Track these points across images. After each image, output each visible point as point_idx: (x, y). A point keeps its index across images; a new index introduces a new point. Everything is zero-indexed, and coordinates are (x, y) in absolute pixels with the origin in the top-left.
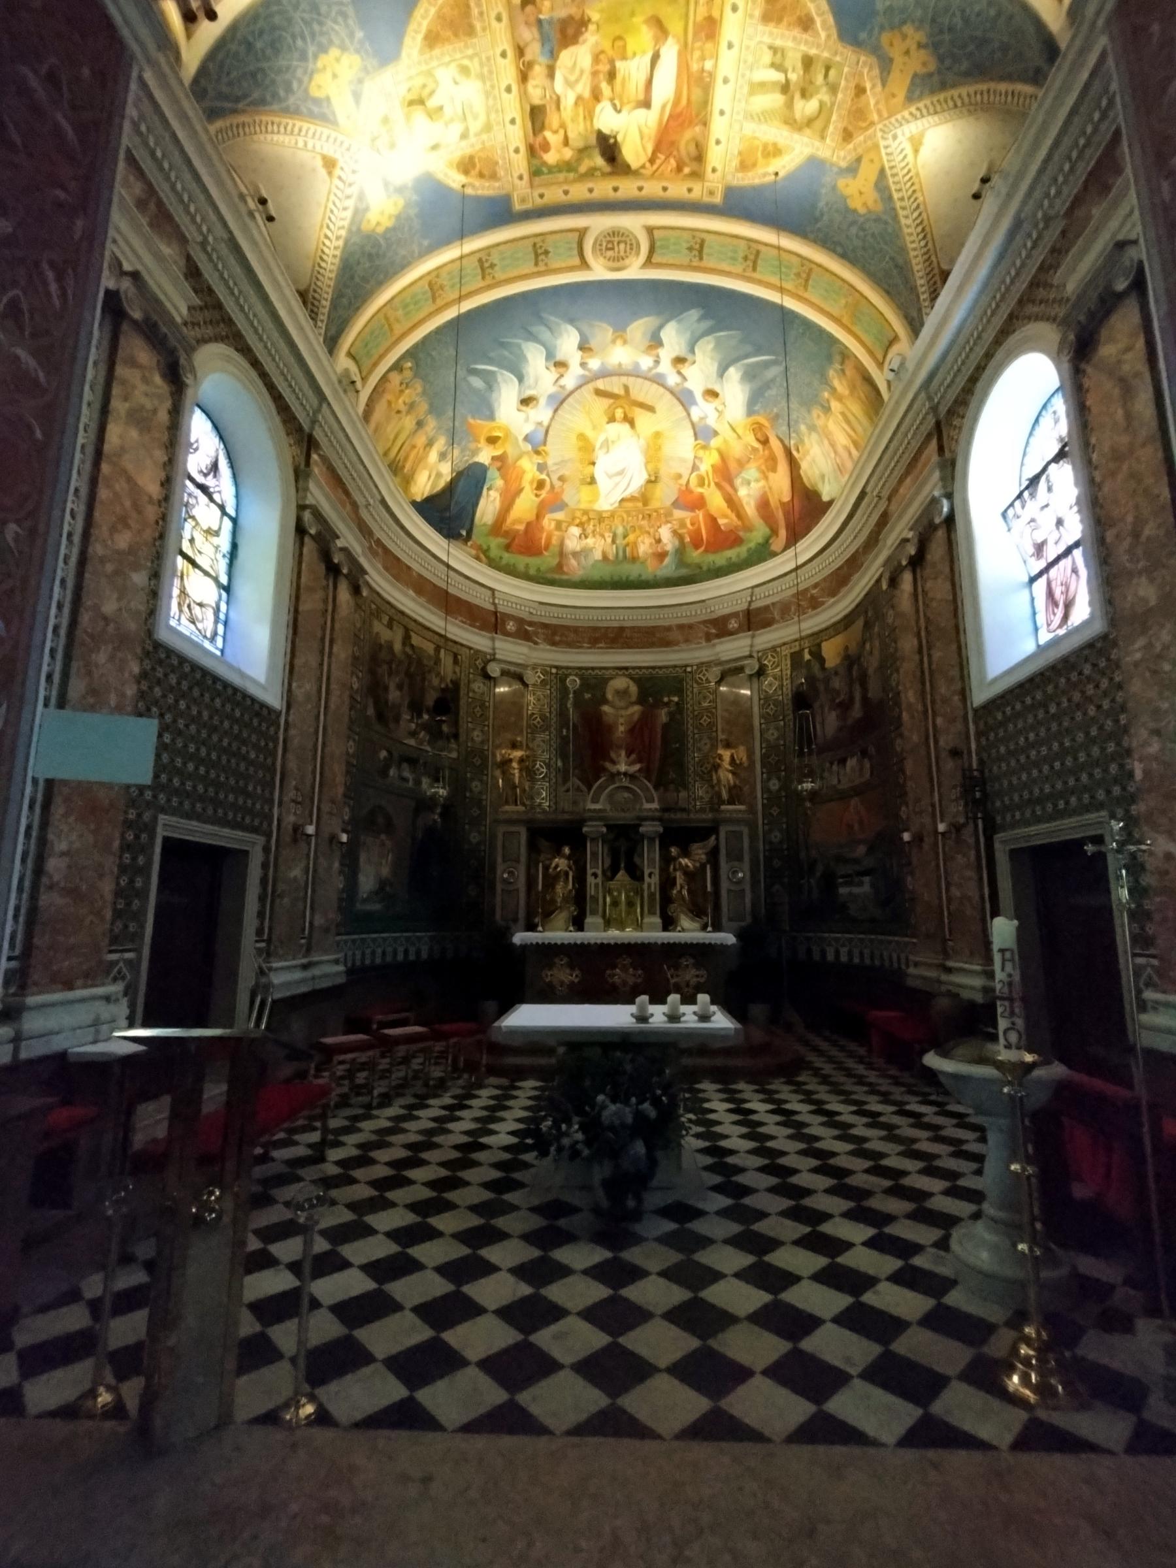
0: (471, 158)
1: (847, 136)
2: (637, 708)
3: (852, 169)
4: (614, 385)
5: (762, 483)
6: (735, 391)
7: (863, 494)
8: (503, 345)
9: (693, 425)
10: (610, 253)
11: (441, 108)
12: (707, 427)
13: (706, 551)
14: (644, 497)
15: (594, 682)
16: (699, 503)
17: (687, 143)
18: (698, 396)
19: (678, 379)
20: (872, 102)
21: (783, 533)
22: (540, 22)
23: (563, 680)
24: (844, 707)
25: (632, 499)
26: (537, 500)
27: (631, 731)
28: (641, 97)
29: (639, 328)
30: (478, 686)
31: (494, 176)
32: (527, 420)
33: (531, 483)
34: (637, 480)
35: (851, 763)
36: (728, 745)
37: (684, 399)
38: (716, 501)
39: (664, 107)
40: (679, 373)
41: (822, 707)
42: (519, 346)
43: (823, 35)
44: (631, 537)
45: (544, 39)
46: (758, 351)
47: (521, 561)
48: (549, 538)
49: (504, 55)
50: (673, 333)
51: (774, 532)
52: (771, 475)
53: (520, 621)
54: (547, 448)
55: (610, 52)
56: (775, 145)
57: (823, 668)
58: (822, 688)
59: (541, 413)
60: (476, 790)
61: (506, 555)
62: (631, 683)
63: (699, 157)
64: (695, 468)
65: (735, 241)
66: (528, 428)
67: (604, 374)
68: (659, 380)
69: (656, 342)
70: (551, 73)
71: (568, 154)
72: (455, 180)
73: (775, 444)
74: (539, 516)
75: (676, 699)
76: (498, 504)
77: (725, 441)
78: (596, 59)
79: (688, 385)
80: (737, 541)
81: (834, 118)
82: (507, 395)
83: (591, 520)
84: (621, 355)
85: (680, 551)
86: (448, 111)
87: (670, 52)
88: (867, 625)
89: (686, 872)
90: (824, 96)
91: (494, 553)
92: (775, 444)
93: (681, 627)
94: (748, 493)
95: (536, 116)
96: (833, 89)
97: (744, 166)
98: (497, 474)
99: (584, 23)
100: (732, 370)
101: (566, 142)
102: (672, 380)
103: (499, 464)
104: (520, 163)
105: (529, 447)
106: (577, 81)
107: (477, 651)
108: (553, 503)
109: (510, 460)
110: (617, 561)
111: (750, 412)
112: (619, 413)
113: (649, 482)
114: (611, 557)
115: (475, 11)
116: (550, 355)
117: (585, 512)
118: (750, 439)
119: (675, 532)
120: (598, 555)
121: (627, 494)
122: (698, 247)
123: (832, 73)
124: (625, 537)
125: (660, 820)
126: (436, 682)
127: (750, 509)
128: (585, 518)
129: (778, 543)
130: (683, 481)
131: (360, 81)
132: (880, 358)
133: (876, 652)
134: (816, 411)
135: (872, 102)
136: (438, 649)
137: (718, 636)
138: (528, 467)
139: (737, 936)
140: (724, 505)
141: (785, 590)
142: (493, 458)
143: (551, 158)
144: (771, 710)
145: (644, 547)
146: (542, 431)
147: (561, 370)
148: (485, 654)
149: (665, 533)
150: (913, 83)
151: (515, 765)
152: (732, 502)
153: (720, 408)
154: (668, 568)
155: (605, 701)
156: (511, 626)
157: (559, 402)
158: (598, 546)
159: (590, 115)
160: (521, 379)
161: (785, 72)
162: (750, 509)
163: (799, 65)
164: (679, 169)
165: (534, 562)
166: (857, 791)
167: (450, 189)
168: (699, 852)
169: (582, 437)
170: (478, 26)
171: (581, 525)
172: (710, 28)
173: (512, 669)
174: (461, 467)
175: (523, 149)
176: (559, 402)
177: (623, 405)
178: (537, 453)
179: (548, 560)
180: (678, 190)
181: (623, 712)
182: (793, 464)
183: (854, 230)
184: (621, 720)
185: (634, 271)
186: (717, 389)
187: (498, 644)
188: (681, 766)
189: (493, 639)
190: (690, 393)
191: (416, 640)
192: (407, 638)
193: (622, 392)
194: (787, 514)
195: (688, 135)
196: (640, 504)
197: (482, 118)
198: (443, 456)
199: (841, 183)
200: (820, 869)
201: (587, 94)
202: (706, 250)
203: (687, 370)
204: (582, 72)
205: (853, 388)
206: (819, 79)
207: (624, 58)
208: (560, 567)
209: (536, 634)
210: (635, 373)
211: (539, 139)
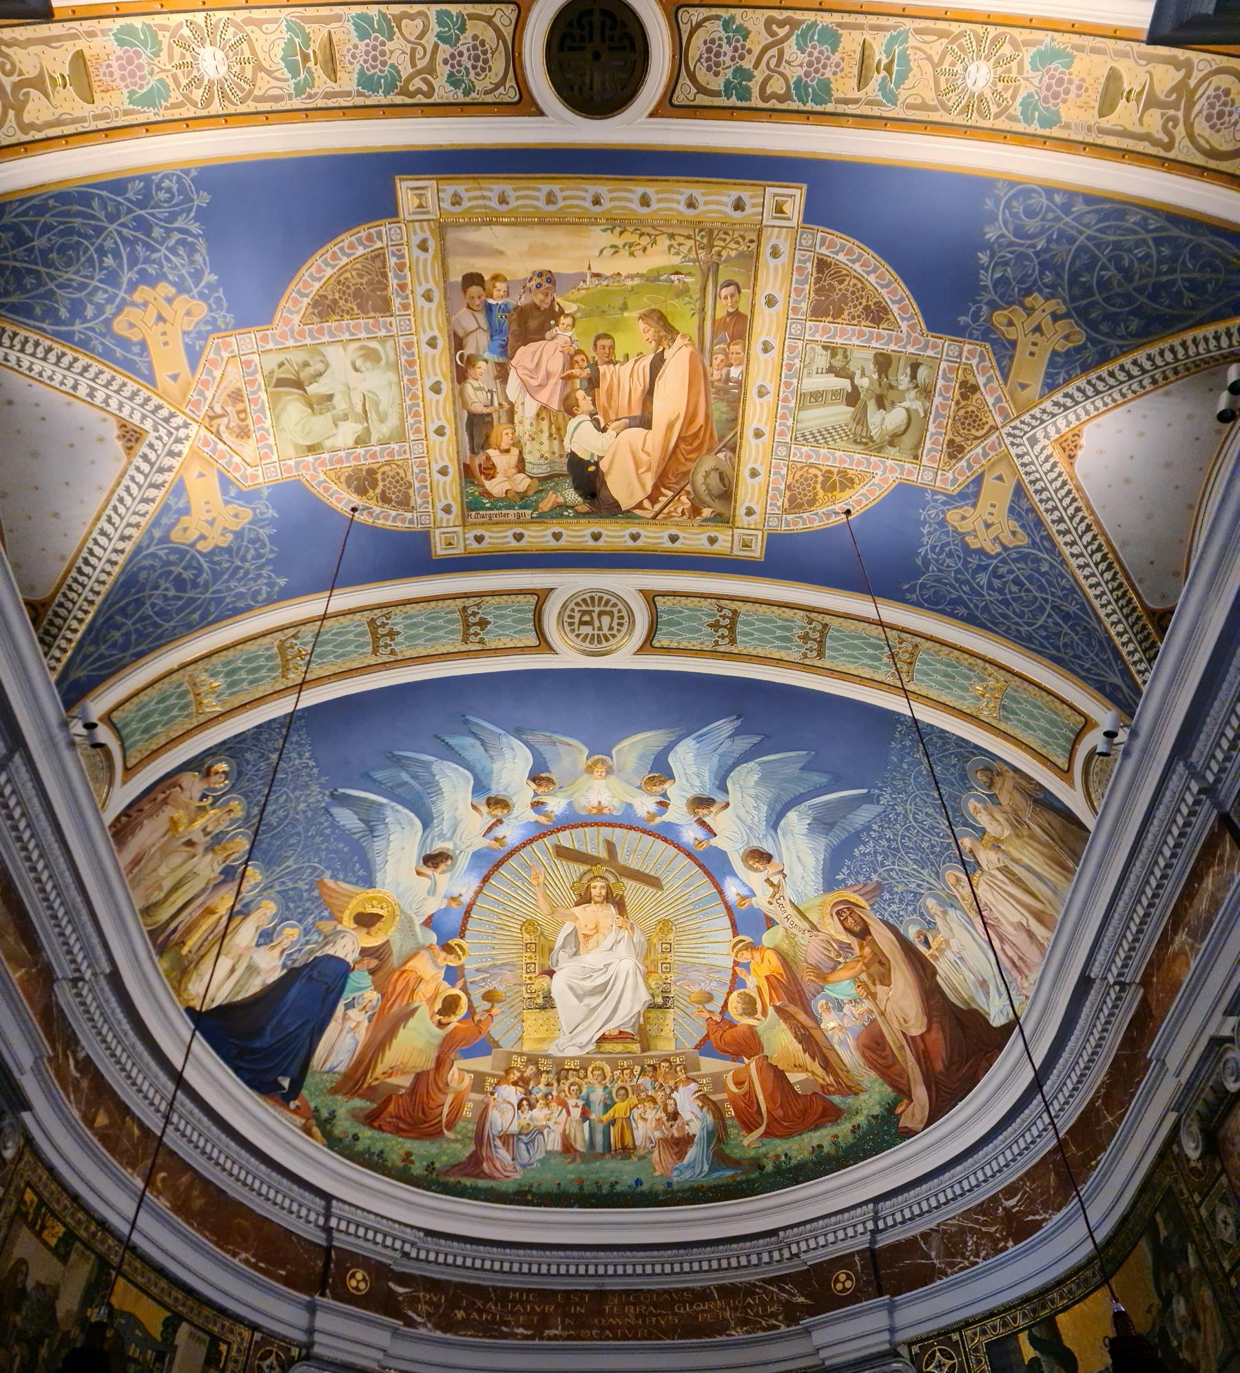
0: (371, 472)
1: (955, 450)
3: (971, 494)
4: (590, 841)
5: (867, 1004)
6: (800, 851)
7: (1085, 982)
8: (399, 762)
9: (729, 909)
10: (585, 630)
11: (330, 397)
12: (754, 912)
13: (766, 1134)
14: (642, 1035)
16: (746, 1046)
17: (707, 475)
19: (700, 833)
20: (990, 400)
21: (920, 1093)
22: (489, 309)
25: (622, 1036)
26: (442, 1033)
28: (637, 412)
29: (634, 748)
31: (405, 503)
32: (432, 891)
34: (630, 1003)
37: (712, 866)
38: (780, 1041)
39: (670, 426)
40: (702, 823)
42: (426, 765)
43: (904, 326)
44: (620, 1109)
45: (494, 331)
46: (838, 782)
47: (396, 1146)
49: (432, 343)
50: (690, 757)
51: (903, 1092)
52: (880, 990)
53: (379, 1271)
55: (591, 353)
56: (843, 473)
59: (458, 882)
61: (366, 1133)
63: (727, 495)
64: (736, 982)
65: (789, 613)
66: (433, 906)
67: (571, 822)
68: (666, 834)
69: (660, 771)
70: (502, 374)
71: (522, 483)
72: (342, 499)
73: (882, 936)
74: (441, 1063)
76: (362, 1035)
77: (788, 936)
78: (571, 361)
80: (832, 1114)
81: (932, 428)
82: (400, 845)
83: (541, 1075)
84: (601, 793)
85: (717, 1135)
86: (340, 403)
87: (678, 359)
88: (1166, 1260)
90: (913, 402)
92: (882, 936)
93: (727, 1291)
94: (840, 1027)
95: (478, 428)
96: (926, 392)
97: (795, 505)
98: (367, 980)
99: (554, 314)
100: (792, 816)
101: (521, 466)
102: (691, 835)
103: (374, 963)
104: (449, 489)
105: (433, 938)
106: (541, 386)
107: (270, 1336)
108: (473, 1041)
109: (395, 961)
110: (592, 1153)
111: (830, 883)
112: (598, 889)
113: (652, 1006)
114: (580, 1146)
115: (393, 282)
116: (479, 787)
117: (533, 1060)
118: (834, 929)
119: (704, 1099)
120: (553, 1142)
122: (727, 622)
123: (922, 373)
124: (607, 1107)
127: (849, 1055)
128: (530, 1071)
130: (716, 1006)
131: (203, 336)
132: (1062, 762)
133: (1211, 1322)
135: (990, 400)
136: (171, 1325)
137: (813, 1311)
138: (428, 971)
142: (364, 952)
143: (496, 487)
145: (646, 1128)
146: (458, 912)
147: (498, 812)
148: (287, 1342)
149: (686, 1100)
150: (1051, 363)
152: (810, 1041)
153: (775, 880)
156: (358, 1281)
157: (492, 864)
158: (555, 1123)
159: (558, 433)
160: (427, 822)
161: (852, 378)
162: (849, 1055)
163: (871, 367)
164: (695, 511)
167: (332, 511)
169: (530, 925)
170: (396, 303)
171: (522, 1082)
172: (738, 326)
174: (301, 960)
175: (453, 470)
176: (492, 864)
177: (606, 880)
178: (448, 949)
179: (453, 1148)
180: (694, 540)
182: (923, 970)
183: (983, 578)
185: (624, 656)
187: (323, 1321)
189: (312, 1309)
190: (722, 855)
192: (98, 1288)
193: (603, 853)
194: (924, 1058)
195: (708, 463)
196: (636, 1048)
197: (393, 421)
198: (266, 937)
199: (953, 517)
201: (555, 405)
202: (740, 628)
204: (548, 375)
205: (1017, 823)
206: (904, 382)
207: (611, 362)
208: (474, 1164)
209: (413, 1301)
210: (627, 823)
211: (480, 459)
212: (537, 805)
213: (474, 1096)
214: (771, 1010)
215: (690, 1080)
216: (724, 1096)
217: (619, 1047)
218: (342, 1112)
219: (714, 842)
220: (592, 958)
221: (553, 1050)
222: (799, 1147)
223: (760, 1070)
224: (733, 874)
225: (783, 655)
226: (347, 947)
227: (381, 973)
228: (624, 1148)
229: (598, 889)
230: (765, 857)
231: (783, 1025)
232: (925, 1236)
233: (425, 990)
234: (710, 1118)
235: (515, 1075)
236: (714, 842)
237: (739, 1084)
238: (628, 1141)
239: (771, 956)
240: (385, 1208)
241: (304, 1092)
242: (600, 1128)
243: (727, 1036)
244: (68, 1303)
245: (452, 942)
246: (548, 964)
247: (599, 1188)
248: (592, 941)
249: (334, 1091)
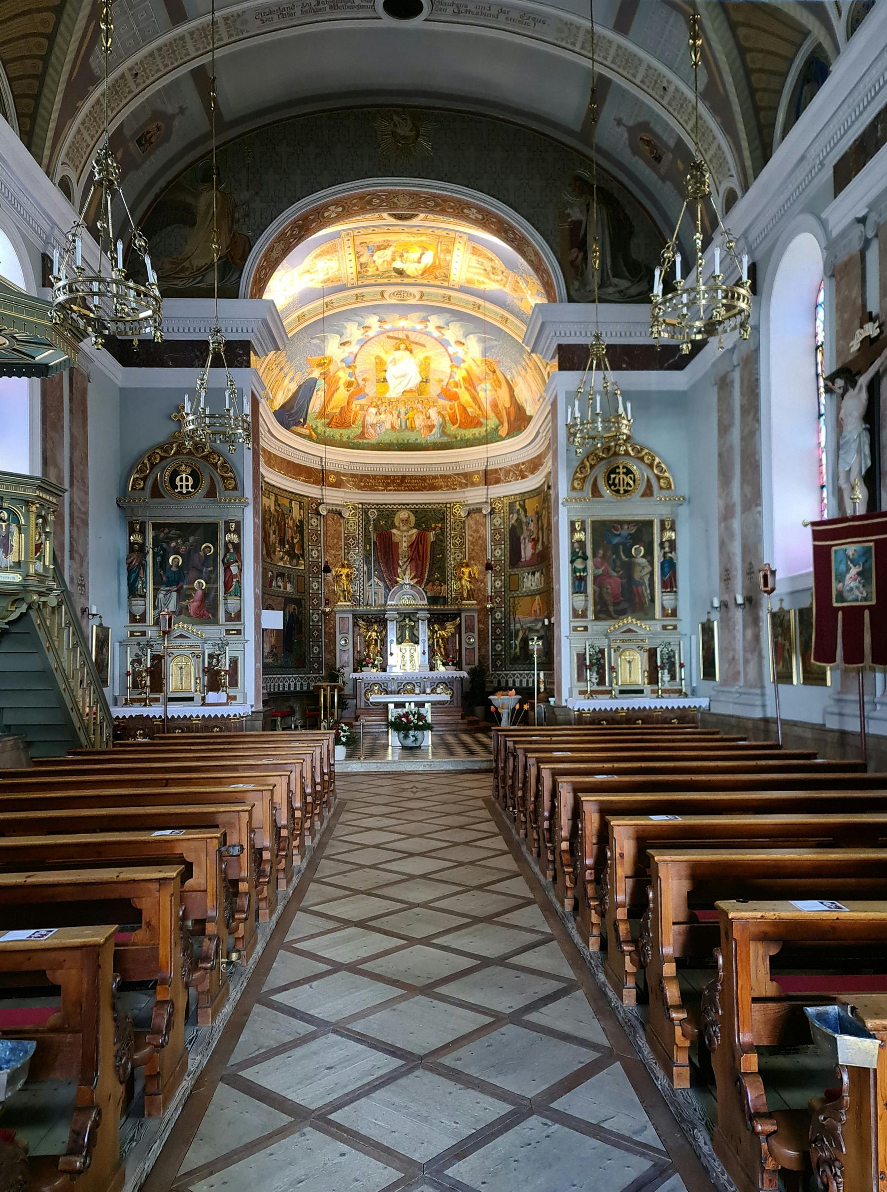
2: (415, 531)
4: (401, 335)
5: (494, 392)
9: (450, 355)
12: (457, 358)
13: (459, 427)
15: (387, 514)
16: (455, 397)
18: (452, 342)
19: (440, 334)
23: (366, 513)
24: (535, 541)
25: (411, 391)
26: (348, 393)
27: (411, 546)
30: (314, 522)
32: (344, 352)
33: (344, 384)
34: (415, 380)
35: (537, 575)
36: (467, 566)
37: (444, 344)
38: (465, 397)
41: (524, 539)
44: (410, 414)
48: (356, 414)
52: (498, 389)
53: (337, 474)
54: (357, 364)
57: (526, 516)
58: (525, 528)
60: (316, 588)
61: (327, 429)
62: (411, 514)
64: (451, 377)
68: (428, 334)
75: (440, 525)
80: (479, 424)
85: (443, 426)
89: (442, 637)
91: (321, 429)
100: (472, 336)
109: (332, 374)
110: (401, 430)
112: (402, 346)
113: (422, 382)
118: (483, 367)
119: (439, 413)
120: (388, 426)
121: (407, 388)
124: (406, 414)
125: (428, 610)
126: (291, 523)
128: (379, 402)
129: (503, 431)
130: (444, 384)
134: (520, 368)
138: (344, 376)
139: (468, 674)
140: (470, 400)
141: (507, 463)
144: (498, 537)
145: (419, 421)
149: (433, 413)
151: (344, 577)
152: (475, 399)
154: (434, 436)
155: (394, 527)
156: (332, 479)
157: (364, 343)
158: (388, 419)
165: (344, 434)
166: (539, 592)
168: (450, 626)
169: (377, 357)
171: (377, 406)
173: (334, 508)
176: (364, 343)
178: (349, 367)
179: (356, 430)
181: (406, 534)
184: (404, 539)
186: (463, 341)
188: (442, 570)
189: (322, 489)
191: (282, 501)
192: (276, 500)
193: (405, 337)
194: (508, 414)
200: (521, 634)
203: (443, 331)
208: (362, 435)
209: (348, 481)
212: (380, 327)
215: (434, 406)
218: (319, 425)
222: (469, 433)
229: (402, 346)
231: (466, 393)
232: (500, 469)
234: (441, 420)
235: (374, 404)
237: (451, 409)
240: (338, 458)
242: (404, 421)
244: (272, 508)
249: (316, 418)
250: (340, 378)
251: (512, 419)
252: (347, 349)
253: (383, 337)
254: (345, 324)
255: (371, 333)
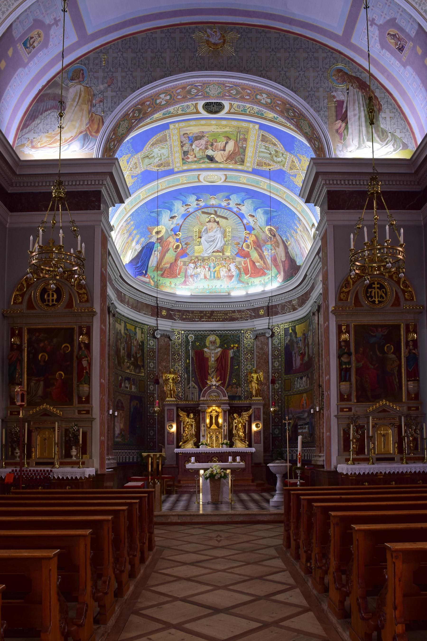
9: (244, 225)
13: (250, 276)
19: (238, 210)
32: (172, 224)
37: (241, 217)
40: (237, 207)
42: (172, 202)
44: (217, 268)
64: (245, 241)
66: (172, 226)
67: (206, 207)
68: (229, 209)
74: (176, 260)
79: (242, 212)
84: (213, 202)
102: (235, 210)
103: (160, 241)
105: (173, 233)
109: (164, 239)
113: (225, 244)
116: (183, 203)
117: (197, 257)
119: (237, 267)
128: (196, 260)
149: (232, 267)
153: (255, 221)
160: (171, 211)
171: (195, 263)
174: (144, 244)
176: (186, 216)
178: (176, 235)
182: (286, 247)
190: (243, 214)
198: (137, 243)
210: (220, 207)
213: (183, 267)
214: (253, 248)
216: (241, 266)
217: (217, 254)
219: (240, 211)
220: (211, 234)
221: (202, 255)
223: (249, 261)
224: (245, 218)
225: (257, 185)
226: (154, 240)
227: (161, 243)
228: (218, 277)
230: (254, 216)
232: (278, 305)
233: (172, 244)
234: (238, 271)
236: (240, 211)
238: (219, 276)
239: (253, 236)
241: (148, 273)
243: (243, 253)
245: (177, 233)
246: (200, 236)
247: (212, 287)
248: (211, 231)
250: (170, 242)
251: (286, 269)
252: (175, 221)
253: (199, 213)
254: (174, 202)
255: (191, 210)
